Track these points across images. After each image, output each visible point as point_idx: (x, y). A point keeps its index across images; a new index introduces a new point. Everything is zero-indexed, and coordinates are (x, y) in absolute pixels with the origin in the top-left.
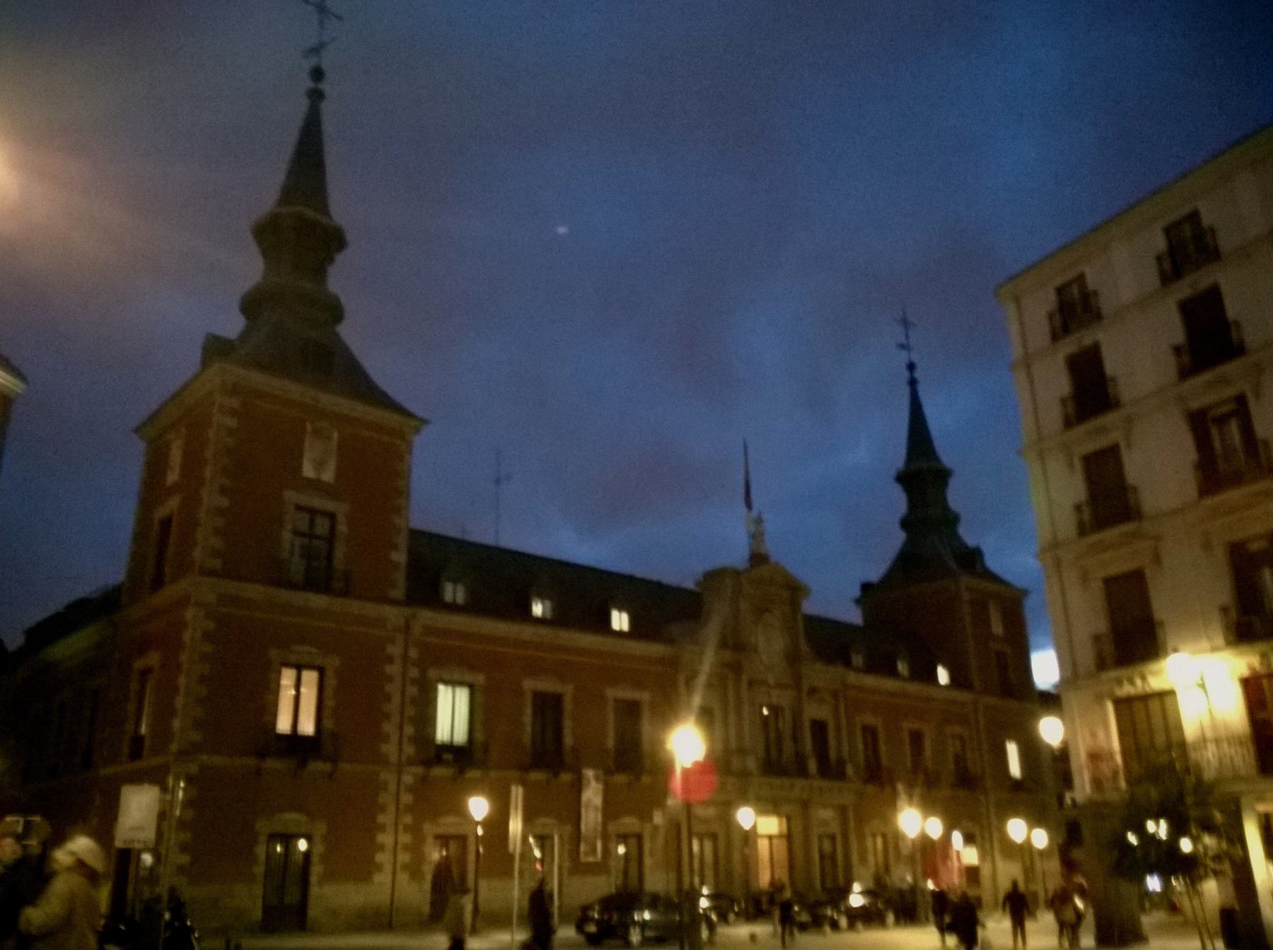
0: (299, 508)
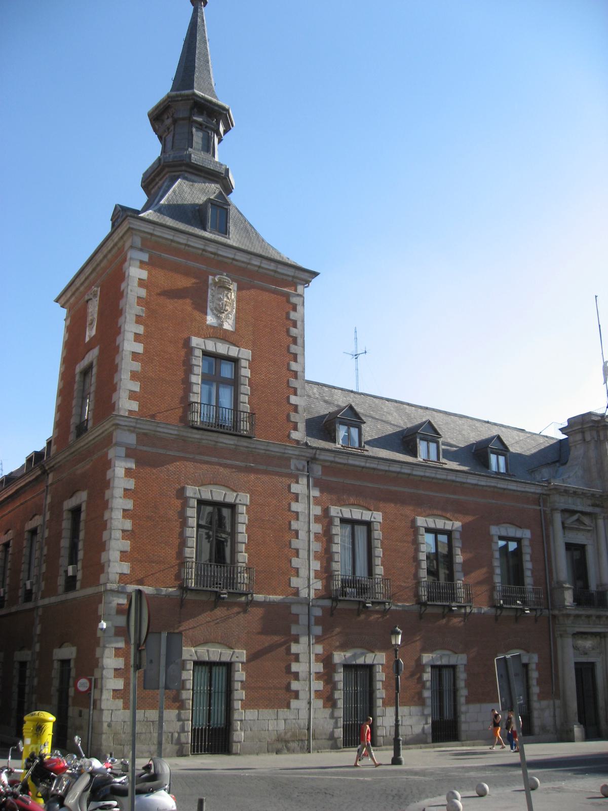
0: (206, 354)
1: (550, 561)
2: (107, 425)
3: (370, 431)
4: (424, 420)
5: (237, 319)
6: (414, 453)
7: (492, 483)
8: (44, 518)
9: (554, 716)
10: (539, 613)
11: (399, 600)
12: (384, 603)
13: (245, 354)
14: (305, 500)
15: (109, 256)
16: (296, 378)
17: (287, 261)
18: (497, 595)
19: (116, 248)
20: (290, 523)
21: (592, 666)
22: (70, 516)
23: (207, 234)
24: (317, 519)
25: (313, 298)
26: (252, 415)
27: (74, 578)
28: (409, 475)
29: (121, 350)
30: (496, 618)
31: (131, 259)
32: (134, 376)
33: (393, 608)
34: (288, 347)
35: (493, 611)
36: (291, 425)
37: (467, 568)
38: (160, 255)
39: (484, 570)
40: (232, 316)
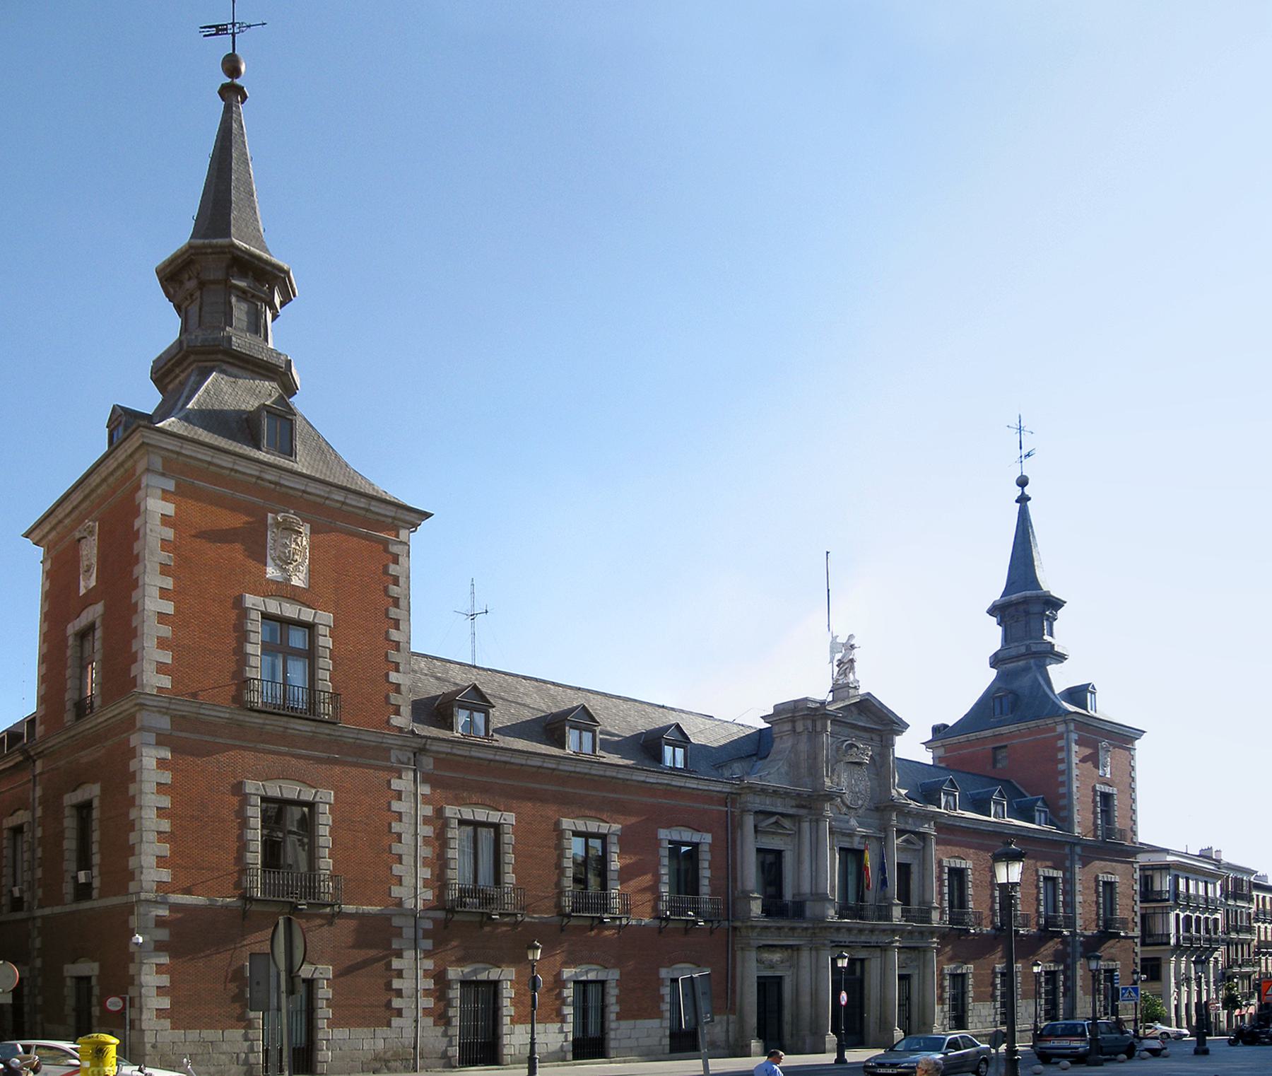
0: (266, 616)
1: (734, 868)
2: (126, 705)
3: (499, 717)
4: (575, 705)
5: (311, 572)
6: (561, 744)
7: (665, 780)
8: (33, 815)
9: (727, 1031)
10: (716, 925)
11: (534, 912)
12: (515, 915)
13: (325, 618)
14: (411, 798)
15: (111, 480)
16: (398, 650)
17: (384, 496)
18: (662, 906)
19: (122, 470)
20: (390, 824)
21: (779, 980)
22: (74, 812)
23: (262, 455)
24: (427, 820)
25: (423, 552)
26: (335, 696)
27: (88, 886)
28: (554, 769)
29: (140, 609)
30: (660, 930)
31: (147, 486)
32: (162, 643)
33: (527, 919)
34: (387, 610)
35: (657, 922)
36: (391, 709)
37: (626, 874)
38: (190, 479)
39: (648, 877)
40: (304, 569)
